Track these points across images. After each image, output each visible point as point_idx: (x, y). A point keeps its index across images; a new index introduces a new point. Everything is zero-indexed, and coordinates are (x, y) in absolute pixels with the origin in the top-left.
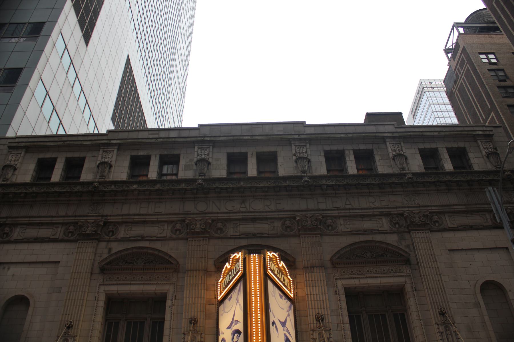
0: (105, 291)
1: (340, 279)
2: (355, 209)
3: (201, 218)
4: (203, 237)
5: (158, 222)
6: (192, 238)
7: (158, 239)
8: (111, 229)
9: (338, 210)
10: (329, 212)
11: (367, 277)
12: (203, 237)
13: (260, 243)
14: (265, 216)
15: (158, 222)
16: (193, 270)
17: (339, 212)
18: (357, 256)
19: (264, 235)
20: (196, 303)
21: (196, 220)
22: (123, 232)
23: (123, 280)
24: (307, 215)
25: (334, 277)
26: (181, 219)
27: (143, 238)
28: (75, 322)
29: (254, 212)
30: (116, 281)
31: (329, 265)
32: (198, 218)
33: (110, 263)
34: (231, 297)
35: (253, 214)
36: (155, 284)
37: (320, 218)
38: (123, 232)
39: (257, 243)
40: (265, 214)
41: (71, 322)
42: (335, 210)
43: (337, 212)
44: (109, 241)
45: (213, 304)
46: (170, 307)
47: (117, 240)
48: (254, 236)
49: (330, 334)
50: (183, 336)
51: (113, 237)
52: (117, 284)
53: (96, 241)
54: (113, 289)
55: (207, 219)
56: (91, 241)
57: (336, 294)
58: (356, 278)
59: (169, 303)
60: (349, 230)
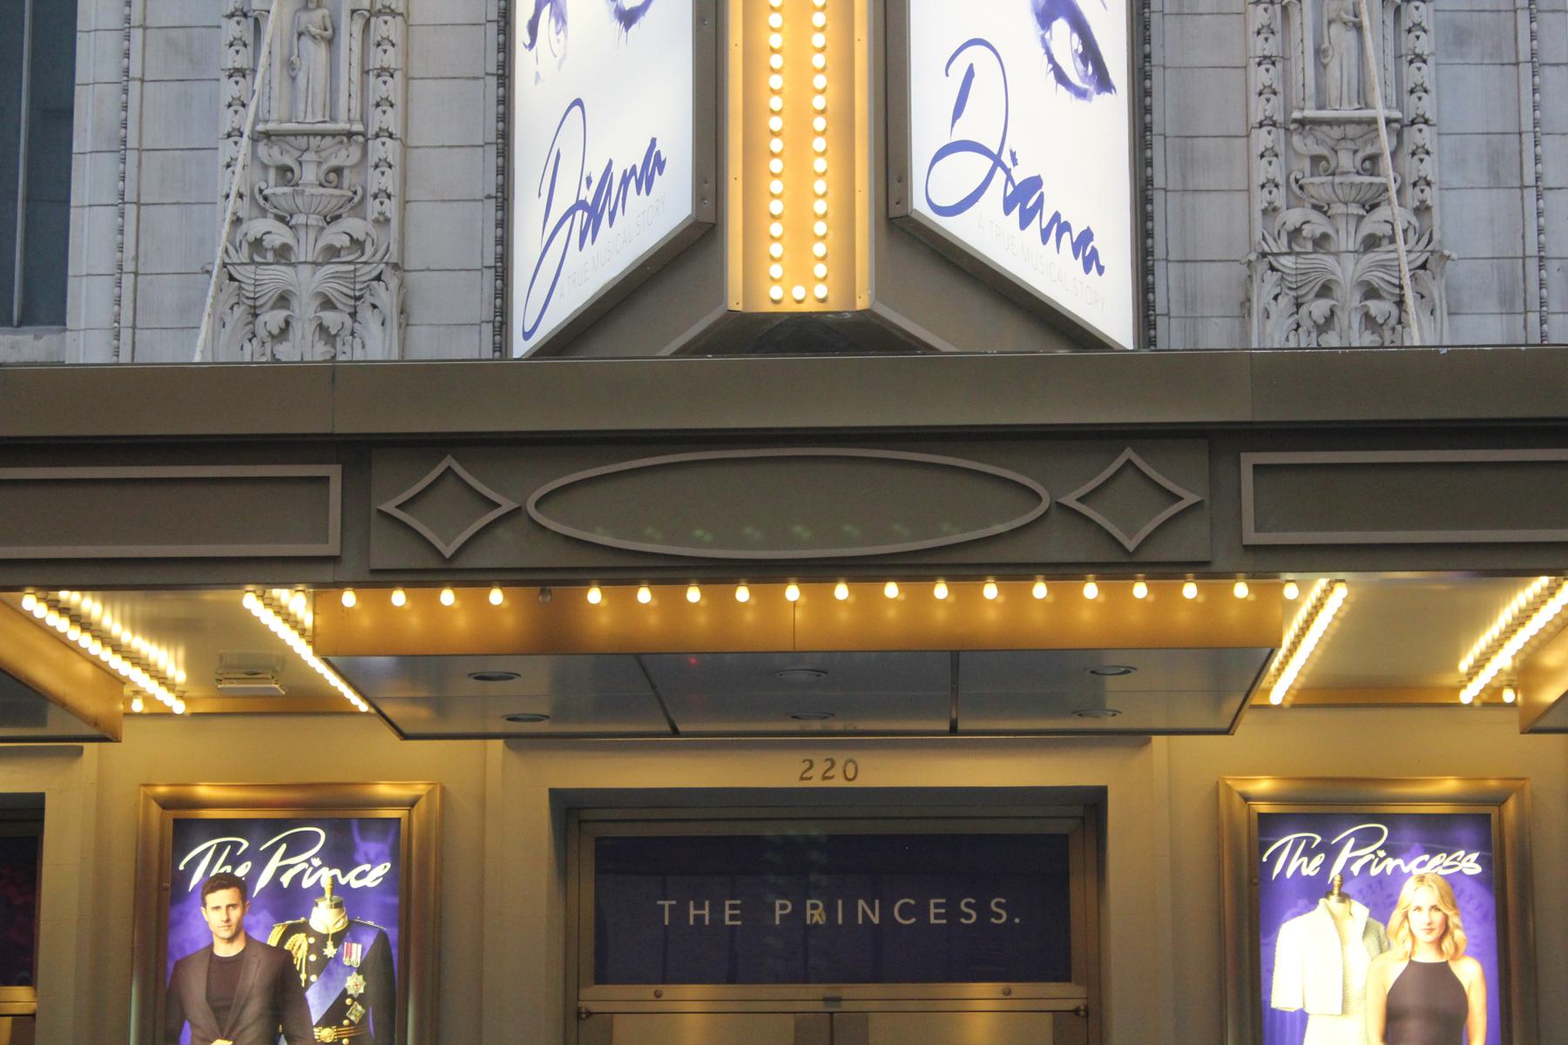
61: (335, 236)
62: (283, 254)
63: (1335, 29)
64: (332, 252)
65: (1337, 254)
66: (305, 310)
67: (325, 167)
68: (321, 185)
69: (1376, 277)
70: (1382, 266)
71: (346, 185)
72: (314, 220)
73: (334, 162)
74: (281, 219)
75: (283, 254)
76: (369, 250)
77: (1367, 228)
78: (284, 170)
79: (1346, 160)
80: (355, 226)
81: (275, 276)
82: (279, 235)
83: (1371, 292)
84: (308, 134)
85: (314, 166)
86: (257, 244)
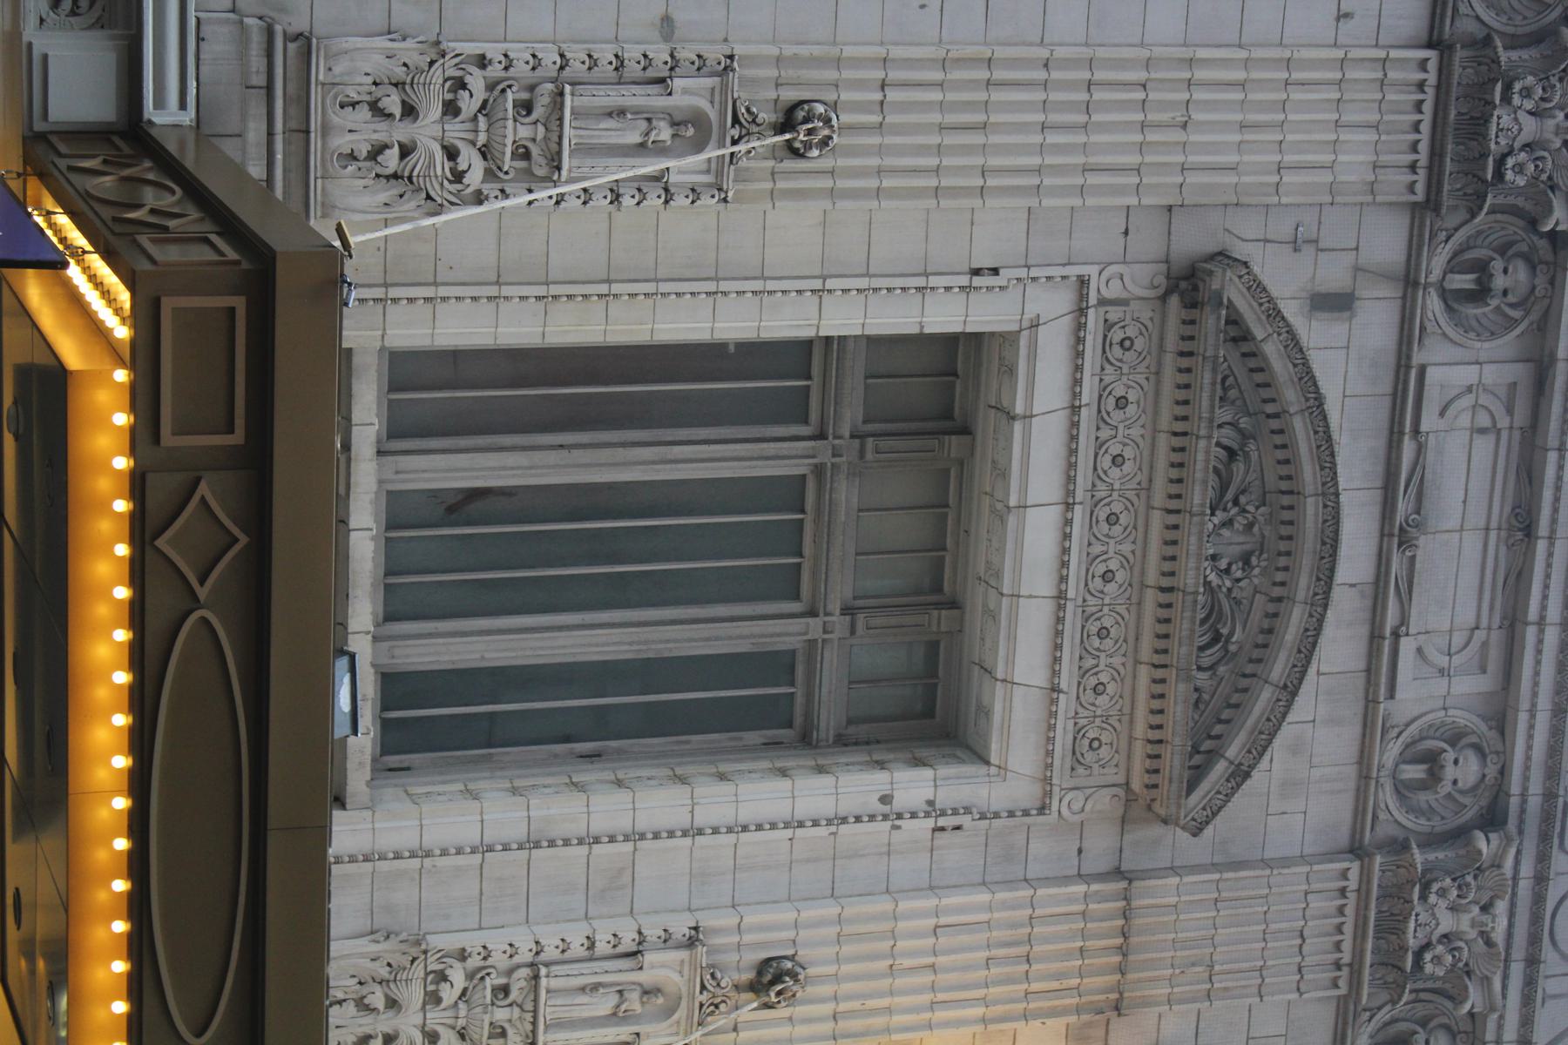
0: (1035, 325)
3: (1499, 936)
4: (1355, 968)
5: (1513, 623)
6: (1363, 892)
7: (1381, 642)
8: (1499, 282)
12: (1355, 968)
15: (1513, 623)
16: (1123, 951)
20: (900, 982)
21: (1485, 909)
22: (1468, 374)
23: (1100, 444)
26: (1515, 789)
27: (1397, 536)
28: (827, 163)
30: (1103, 390)
32: (1502, 923)
33: (1237, 333)
36: (1055, 673)
38: (1468, 374)
41: (825, 142)
44: (1410, 282)
46: (885, 799)
47: (1408, 334)
50: (681, 928)
51: (1434, 303)
52: (1075, 409)
53: (1420, 196)
54: (1044, 386)
55: (1486, 981)
56: (1423, 157)
59: (913, 785)
62: (434, 999)
67: (506, 1026)
72: (461, 1022)
73: (510, 1032)
75: (434, 999)
78: (505, 990)
81: (413, 995)
82: (449, 994)
84: (535, 1012)
85: (507, 1016)
86: (442, 977)
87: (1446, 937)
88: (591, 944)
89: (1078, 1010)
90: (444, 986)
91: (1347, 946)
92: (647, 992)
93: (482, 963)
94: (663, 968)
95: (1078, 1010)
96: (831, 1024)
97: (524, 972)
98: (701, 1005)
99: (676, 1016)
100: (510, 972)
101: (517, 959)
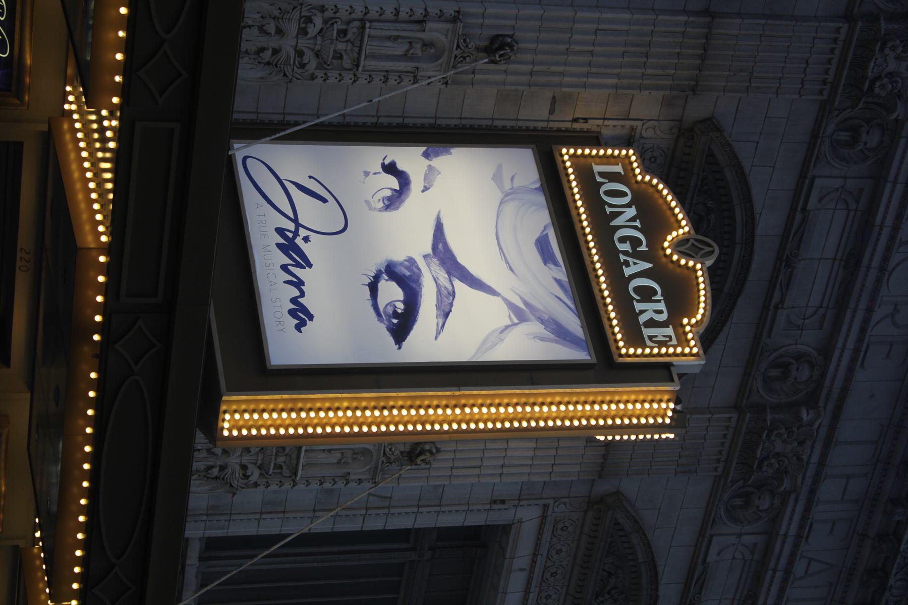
1: (544, 517)
2: (782, 589)
9: (799, 537)
10: (799, 509)
11: (527, 592)
13: (751, 277)
14: (852, 305)
17: (790, 540)
18: (610, 574)
19: (777, 294)
24: (809, 443)
25: (556, 499)
29: (882, 269)
31: (603, 488)
34: (547, 256)
35: (875, 263)
37: (787, 485)
39: (754, 266)
40: (863, 305)
42: (801, 527)
43: (793, 531)
45: (551, 112)
48: (786, 258)
49: (360, 481)
50: (450, 9)
57: (495, 502)
58: (534, 562)
60: (711, 558)
61: (309, 56)
62: (303, 32)
63: (339, 455)
64: (300, 54)
65: (241, 455)
66: (274, 42)
67: (343, 53)
68: (334, 51)
69: (229, 470)
70: (233, 472)
71: (334, 61)
72: (318, 48)
73: (345, 57)
74: (321, 30)
75: (303, 32)
76: (299, 71)
77: (250, 466)
78: (344, 33)
79: (281, 460)
80: (312, 65)
81: (292, 28)
82: (312, 31)
83: (223, 468)
84: (360, 48)
86: (309, 20)
87: (890, 75)
88: (397, 12)
89: (671, 88)
90: (311, 26)
91: (832, 72)
92: (426, 45)
93: (333, 15)
94: (436, 32)
95: (671, 88)
96: (529, 77)
97: (357, 24)
98: (456, 57)
99: (440, 61)
100: (349, 22)
101: (353, 16)
